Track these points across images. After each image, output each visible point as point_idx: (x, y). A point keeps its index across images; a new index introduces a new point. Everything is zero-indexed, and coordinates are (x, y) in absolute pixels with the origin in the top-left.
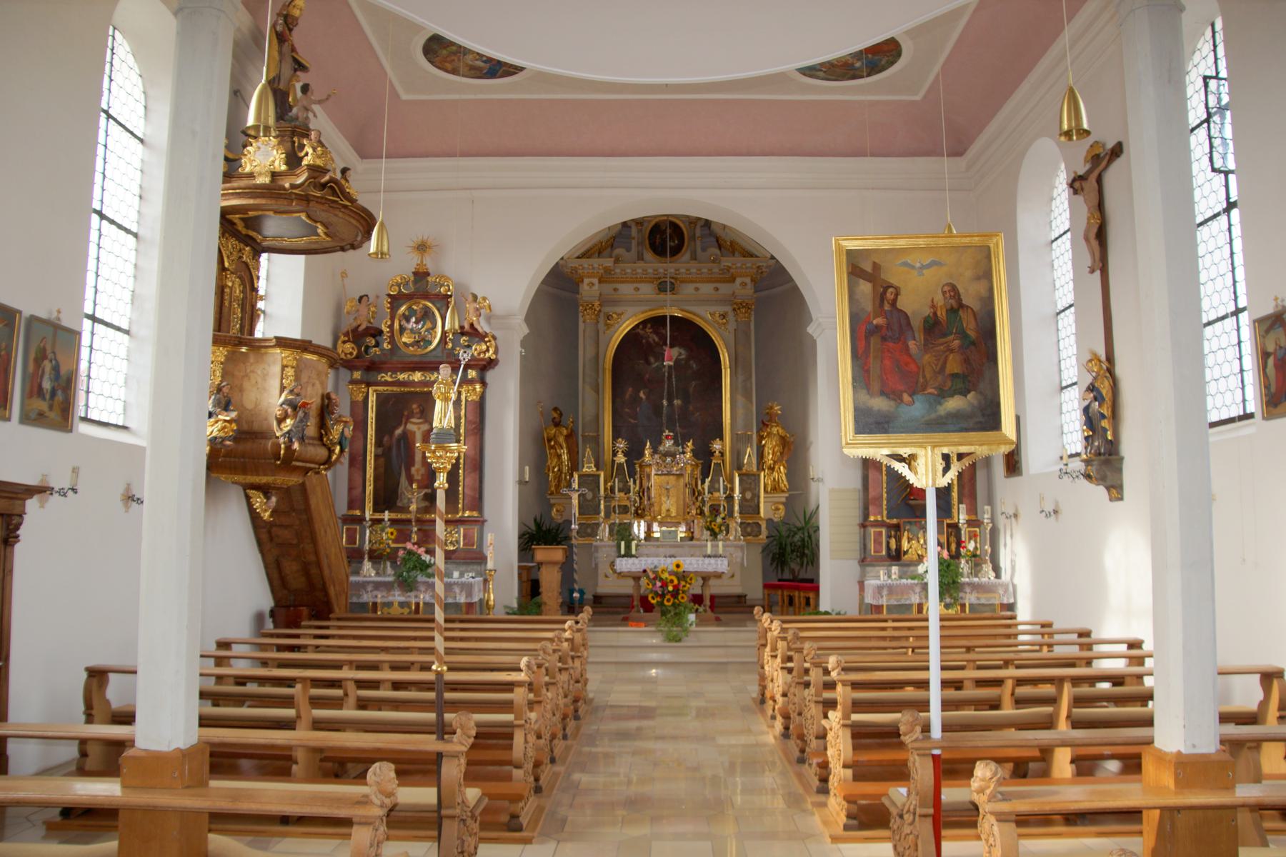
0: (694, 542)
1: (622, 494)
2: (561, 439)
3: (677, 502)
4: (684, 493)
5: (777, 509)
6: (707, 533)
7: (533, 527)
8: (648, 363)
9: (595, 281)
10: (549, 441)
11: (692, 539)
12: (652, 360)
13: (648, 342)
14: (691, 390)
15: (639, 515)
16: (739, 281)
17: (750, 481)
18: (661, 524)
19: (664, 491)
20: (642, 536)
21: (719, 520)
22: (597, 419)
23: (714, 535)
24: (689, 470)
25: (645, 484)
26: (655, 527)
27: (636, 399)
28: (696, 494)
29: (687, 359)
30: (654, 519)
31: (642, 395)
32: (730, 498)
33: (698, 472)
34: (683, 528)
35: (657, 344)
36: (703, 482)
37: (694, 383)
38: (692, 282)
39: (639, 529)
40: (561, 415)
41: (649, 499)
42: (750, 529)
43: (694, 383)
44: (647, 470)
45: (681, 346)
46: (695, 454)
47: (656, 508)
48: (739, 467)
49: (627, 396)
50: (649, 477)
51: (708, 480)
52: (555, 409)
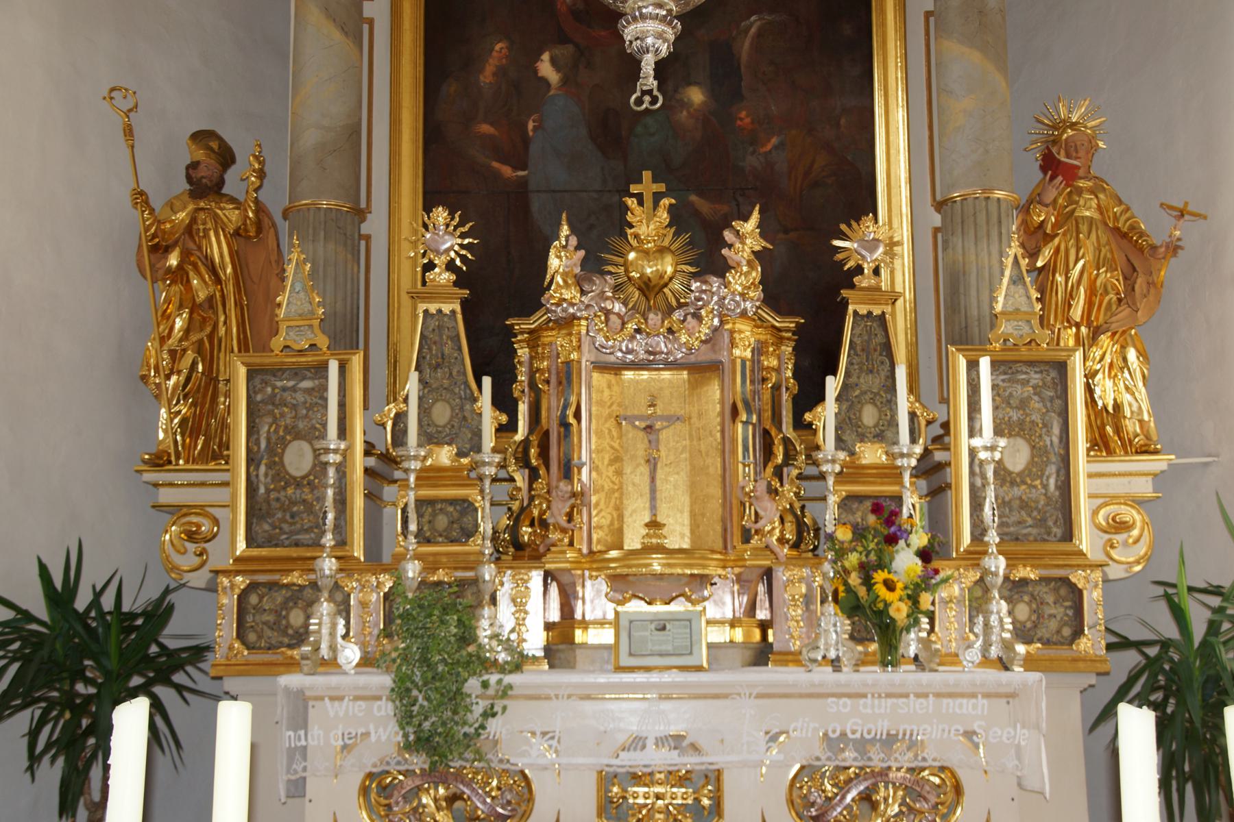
0: (771, 675)
1: (444, 456)
2: (218, 248)
3: (693, 487)
5: (1120, 526)
6: (834, 626)
7: (38, 606)
10: (160, 249)
11: (762, 654)
14: (745, 47)
15: (517, 550)
17: (1035, 385)
18: (622, 585)
19: (638, 443)
20: (535, 641)
21: (906, 562)
22: (351, 139)
23: (876, 629)
24: (746, 338)
25: (550, 419)
26: (594, 601)
27: (521, 87)
28: (780, 445)
30: (594, 559)
31: (546, 68)
32: (933, 472)
33: (782, 363)
34: (723, 603)
36: (810, 395)
37: (755, 23)
39: (520, 611)
40: (226, 158)
41: (567, 471)
42: (1051, 610)
43: (755, 23)
44: (559, 340)
46: (775, 295)
47: (599, 517)
48: (960, 327)
49: (487, 77)
50: (567, 376)
51: (832, 385)
52: (200, 137)
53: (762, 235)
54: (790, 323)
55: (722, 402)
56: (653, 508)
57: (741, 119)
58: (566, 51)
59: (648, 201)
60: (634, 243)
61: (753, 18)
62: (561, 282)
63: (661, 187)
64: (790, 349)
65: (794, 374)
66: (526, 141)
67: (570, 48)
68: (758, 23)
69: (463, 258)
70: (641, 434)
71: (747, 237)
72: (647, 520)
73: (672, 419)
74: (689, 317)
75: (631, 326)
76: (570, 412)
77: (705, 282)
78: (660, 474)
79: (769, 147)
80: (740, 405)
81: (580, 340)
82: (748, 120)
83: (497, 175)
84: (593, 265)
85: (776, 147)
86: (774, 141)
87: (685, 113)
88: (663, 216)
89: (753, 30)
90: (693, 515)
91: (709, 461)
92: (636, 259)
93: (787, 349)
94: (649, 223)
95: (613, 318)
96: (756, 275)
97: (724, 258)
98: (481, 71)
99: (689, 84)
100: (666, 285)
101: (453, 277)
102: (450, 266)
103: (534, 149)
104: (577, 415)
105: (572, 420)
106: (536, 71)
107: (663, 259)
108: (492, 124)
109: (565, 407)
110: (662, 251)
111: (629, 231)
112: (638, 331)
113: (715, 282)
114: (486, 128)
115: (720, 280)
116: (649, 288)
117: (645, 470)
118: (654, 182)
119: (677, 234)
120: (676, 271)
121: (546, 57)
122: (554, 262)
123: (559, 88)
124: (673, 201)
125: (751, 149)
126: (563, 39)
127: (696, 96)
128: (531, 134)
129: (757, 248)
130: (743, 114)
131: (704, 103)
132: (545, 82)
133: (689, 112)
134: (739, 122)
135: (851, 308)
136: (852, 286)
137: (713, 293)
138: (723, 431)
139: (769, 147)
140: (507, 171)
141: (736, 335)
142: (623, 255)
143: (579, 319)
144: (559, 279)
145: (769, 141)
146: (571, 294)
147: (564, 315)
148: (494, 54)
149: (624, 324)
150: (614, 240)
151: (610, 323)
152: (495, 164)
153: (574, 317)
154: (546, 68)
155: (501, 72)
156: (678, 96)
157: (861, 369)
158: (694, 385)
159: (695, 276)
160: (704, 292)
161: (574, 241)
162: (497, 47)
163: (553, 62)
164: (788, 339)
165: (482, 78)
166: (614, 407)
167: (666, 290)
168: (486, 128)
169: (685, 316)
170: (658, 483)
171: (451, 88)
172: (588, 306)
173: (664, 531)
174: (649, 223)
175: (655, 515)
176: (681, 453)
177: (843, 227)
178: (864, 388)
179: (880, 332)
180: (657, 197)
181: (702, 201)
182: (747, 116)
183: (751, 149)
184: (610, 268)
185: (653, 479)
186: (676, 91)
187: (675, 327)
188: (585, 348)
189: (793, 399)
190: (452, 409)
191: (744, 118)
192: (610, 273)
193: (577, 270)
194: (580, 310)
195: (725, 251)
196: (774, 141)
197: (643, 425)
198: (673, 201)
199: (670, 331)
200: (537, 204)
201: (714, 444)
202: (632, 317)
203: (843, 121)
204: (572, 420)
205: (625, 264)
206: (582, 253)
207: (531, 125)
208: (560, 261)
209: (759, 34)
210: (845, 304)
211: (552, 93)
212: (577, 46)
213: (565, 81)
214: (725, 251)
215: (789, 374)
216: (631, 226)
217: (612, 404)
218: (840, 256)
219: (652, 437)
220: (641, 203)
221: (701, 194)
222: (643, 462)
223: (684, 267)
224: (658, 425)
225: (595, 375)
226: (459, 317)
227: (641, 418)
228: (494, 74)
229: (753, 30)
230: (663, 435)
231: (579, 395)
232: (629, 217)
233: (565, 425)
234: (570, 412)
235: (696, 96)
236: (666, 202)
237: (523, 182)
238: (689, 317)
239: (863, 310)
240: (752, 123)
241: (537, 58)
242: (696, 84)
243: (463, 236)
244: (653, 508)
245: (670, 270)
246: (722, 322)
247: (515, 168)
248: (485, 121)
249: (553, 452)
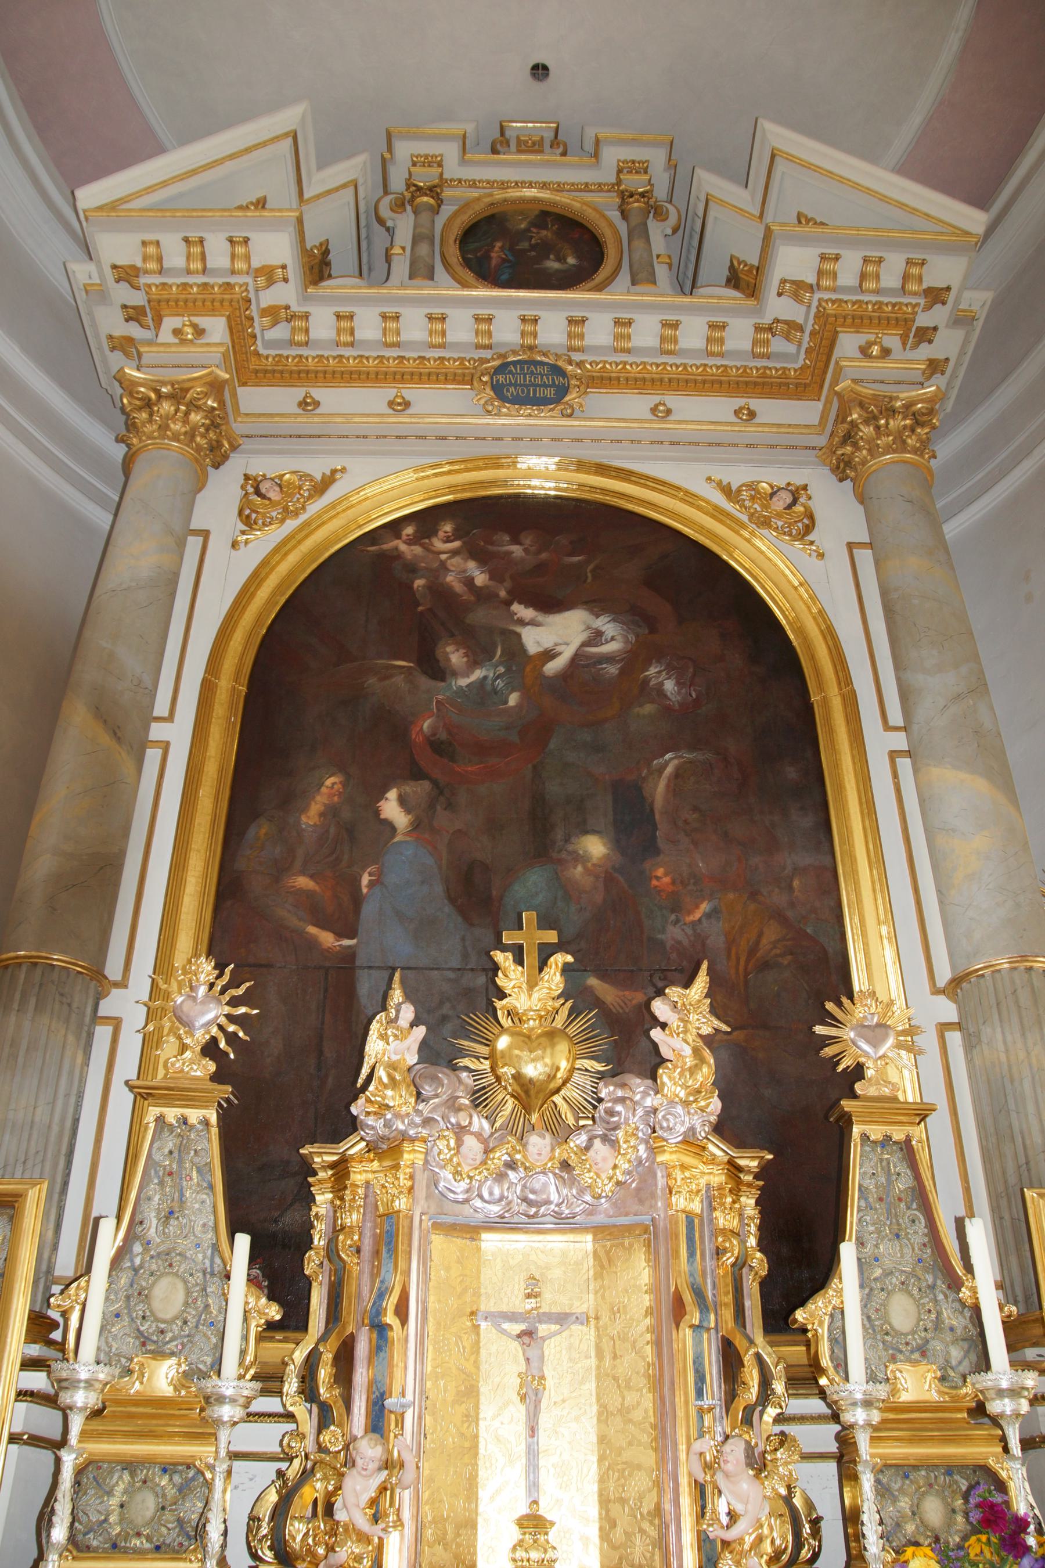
4: (661, 1383)
8: (438, 671)
9: (217, 328)
12: (456, 657)
13: (440, 593)
14: (659, 790)
16: (848, 343)
27: (357, 833)
29: (633, 660)
31: (391, 808)
35: (483, 596)
37: (671, 762)
38: (641, 383)
43: (671, 762)
45: (596, 604)
49: (311, 817)
50: (389, 1236)
53: (714, 1011)
54: (750, 1162)
55: (655, 1289)
56: (533, 1486)
57: (658, 878)
58: (420, 789)
59: (531, 958)
60: (506, 1022)
61: (668, 756)
62: (385, 1080)
63: (551, 937)
64: (752, 1202)
65: (758, 1244)
66: (357, 900)
67: (426, 785)
68: (676, 762)
69: (231, 1038)
70: (515, 1346)
71: (685, 1018)
72: (524, 1510)
73: (562, 1319)
74: (597, 1142)
75: (501, 1156)
76: (391, 1303)
77: (623, 1085)
78: (544, 1420)
79: (697, 915)
80: (688, 1297)
81: (412, 1177)
82: (667, 880)
83: (313, 944)
84: (438, 1054)
85: (708, 915)
86: (705, 907)
87: (580, 869)
88: (553, 979)
89: (669, 770)
90: (604, 1501)
91: (631, 1398)
92: (510, 1047)
93: (749, 1202)
94: (531, 989)
95: (470, 1141)
96: (706, 1074)
97: (655, 1046)
98: (305, 809)
99: (586, 832)
100: (557, 1091)
101: (212, 1067)
102: (210, 1049)
103: (368, 910)
104: (402, 1310)
105: (390, 1318)
106: (377, 812)
107: (553, 1045)
108: (312, 877)
109: (381, 1296)
110: (551, 1035)
111: (498, 1004)
112: (511, 1165)
113: (638, 1085)
114: (303, 882)
115: (649, 1082)
116: (528, 1094)
117: (519, 1411)
118: (540, 927)
119: (574, 1013)
120: (572, 1070)
121: (392, 794)
122: (374, 1046)
123: (408, 834)
124: (569, 958)
125: (673, 917)
126: (417, 774)
127: (595, 847)
128: (365, 890)
129: (706, 1030)
130: (660, 872)
131: (606, 857)
132: (390, 827)
133: (585, 868)
134: (654, 882)
135: (856, 1130)
136: (854, 1096)
137: (635, 1103)
138: (658, 1344)
139: (697, 915)
140: (327, 939)
141: (678, 1174)
142: (488, 1043)
143: (412, 1140)
144: (381, 1073)
145: (697, 907)
146: (399, 1099)
147: (387, 1132)
148: (324, 790)
149: (487, 1151)
150: (477, 1019)
151: (463, 1149)
152: (312, 930)
153: (404, 1137)
154: (391, 808)
155: (331, 812)
156: (570, 848)
157: (878, 1232)
158: (604, 1263)
159: (602, 1076)
160: (622, 1100)
161: (408, 1013)
162: (329, 782)
163: (402, 801)
164: (749, 1185)
165: (304, 819)
166: (468, 1298)
167: (557, 1099)
168: (303, 882)
169: (591, 1140)
170: (541, 1433)
171: (261, 830)
172: (427, 1122)
173: (553, 1536)
174: (531, 989)
175: (535, 1502)
176: (582, 1382)
177: (830, 1006)
178: (888, 1263)
179: (902, 1168)
180: (545, 953)
181: (606, 986)
182: (666, 875)
183: (673, 917)
184: (466, 1062)
185: (533, 1431)
186: (567, 840)
187: (573, 1160)
188: (421, 1192)
189: (761, 1284)
190: (188, 1293)
191: (661, 876)
192: (467, 1069)
193: (412, 1059)
194: (412, 1124)
195: (656, 1034)
196: (705, 907)
197: (517, 1328)
198: (569, 958)
199: (565, 1165)
200: (365, 985)
201: (641, 1366)
202: (502, 1141)
203: (796, 883)
204: (390, 1318)
205: (492, 1057)
206: (421, 1031)
207: (365, 879)
208: (392, 1043)
209: (677, 775)
210: (846, 1121)
211: (396, 840)
212: (435, 783)
213: (416, 826)
214: (656, 1034)
215: (752, 1241)
216: (502, 995)
217: (465, 1290)
218: (828, 1051)
219: (532, 1353)
220: (519, 961)
221: (603, 975)
222: (517, 1399)
223: (588, 1064)
224: (543, 1329)
225: (438, 1241)
226: (215, 1131)
227: (512, 1317)
228: (322, 815)
229: (669, 770)
230: (551, 1348)
231: (408, 1273)
232: (501, 981)
233: (380, 1329)
234: (391, 1303)
235: (595, 847)
236: (561, 959)
237: (349, 957)
238: (597, 1142)
239: (876, 1132)
240: (673, 883)
241: (381, 794)
242: (594, 832)
243: (234, 1002)
244: (533, 1486)
245: (564, 1065)
246: (653, 1151)
247: (340, 935)
248: (303, 873)
249: (361, 1376)
